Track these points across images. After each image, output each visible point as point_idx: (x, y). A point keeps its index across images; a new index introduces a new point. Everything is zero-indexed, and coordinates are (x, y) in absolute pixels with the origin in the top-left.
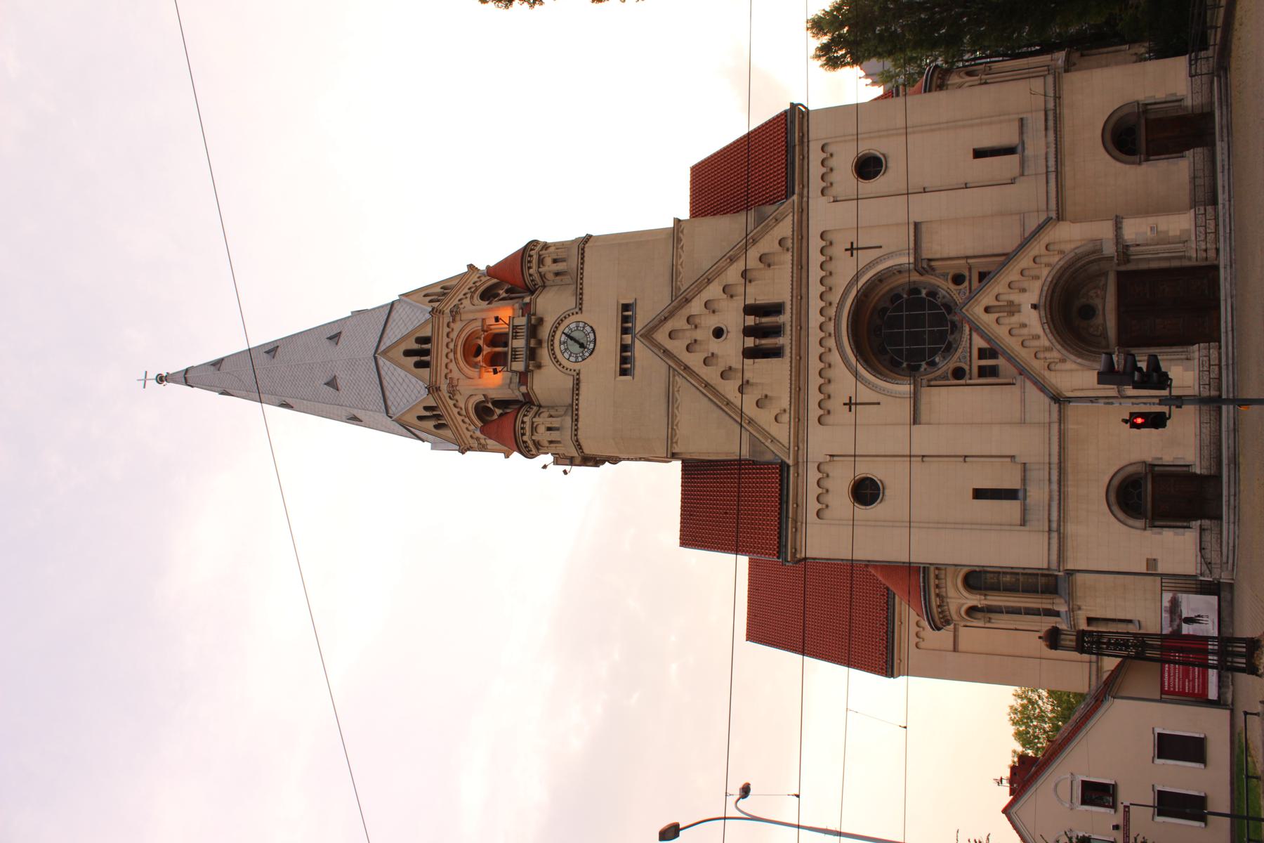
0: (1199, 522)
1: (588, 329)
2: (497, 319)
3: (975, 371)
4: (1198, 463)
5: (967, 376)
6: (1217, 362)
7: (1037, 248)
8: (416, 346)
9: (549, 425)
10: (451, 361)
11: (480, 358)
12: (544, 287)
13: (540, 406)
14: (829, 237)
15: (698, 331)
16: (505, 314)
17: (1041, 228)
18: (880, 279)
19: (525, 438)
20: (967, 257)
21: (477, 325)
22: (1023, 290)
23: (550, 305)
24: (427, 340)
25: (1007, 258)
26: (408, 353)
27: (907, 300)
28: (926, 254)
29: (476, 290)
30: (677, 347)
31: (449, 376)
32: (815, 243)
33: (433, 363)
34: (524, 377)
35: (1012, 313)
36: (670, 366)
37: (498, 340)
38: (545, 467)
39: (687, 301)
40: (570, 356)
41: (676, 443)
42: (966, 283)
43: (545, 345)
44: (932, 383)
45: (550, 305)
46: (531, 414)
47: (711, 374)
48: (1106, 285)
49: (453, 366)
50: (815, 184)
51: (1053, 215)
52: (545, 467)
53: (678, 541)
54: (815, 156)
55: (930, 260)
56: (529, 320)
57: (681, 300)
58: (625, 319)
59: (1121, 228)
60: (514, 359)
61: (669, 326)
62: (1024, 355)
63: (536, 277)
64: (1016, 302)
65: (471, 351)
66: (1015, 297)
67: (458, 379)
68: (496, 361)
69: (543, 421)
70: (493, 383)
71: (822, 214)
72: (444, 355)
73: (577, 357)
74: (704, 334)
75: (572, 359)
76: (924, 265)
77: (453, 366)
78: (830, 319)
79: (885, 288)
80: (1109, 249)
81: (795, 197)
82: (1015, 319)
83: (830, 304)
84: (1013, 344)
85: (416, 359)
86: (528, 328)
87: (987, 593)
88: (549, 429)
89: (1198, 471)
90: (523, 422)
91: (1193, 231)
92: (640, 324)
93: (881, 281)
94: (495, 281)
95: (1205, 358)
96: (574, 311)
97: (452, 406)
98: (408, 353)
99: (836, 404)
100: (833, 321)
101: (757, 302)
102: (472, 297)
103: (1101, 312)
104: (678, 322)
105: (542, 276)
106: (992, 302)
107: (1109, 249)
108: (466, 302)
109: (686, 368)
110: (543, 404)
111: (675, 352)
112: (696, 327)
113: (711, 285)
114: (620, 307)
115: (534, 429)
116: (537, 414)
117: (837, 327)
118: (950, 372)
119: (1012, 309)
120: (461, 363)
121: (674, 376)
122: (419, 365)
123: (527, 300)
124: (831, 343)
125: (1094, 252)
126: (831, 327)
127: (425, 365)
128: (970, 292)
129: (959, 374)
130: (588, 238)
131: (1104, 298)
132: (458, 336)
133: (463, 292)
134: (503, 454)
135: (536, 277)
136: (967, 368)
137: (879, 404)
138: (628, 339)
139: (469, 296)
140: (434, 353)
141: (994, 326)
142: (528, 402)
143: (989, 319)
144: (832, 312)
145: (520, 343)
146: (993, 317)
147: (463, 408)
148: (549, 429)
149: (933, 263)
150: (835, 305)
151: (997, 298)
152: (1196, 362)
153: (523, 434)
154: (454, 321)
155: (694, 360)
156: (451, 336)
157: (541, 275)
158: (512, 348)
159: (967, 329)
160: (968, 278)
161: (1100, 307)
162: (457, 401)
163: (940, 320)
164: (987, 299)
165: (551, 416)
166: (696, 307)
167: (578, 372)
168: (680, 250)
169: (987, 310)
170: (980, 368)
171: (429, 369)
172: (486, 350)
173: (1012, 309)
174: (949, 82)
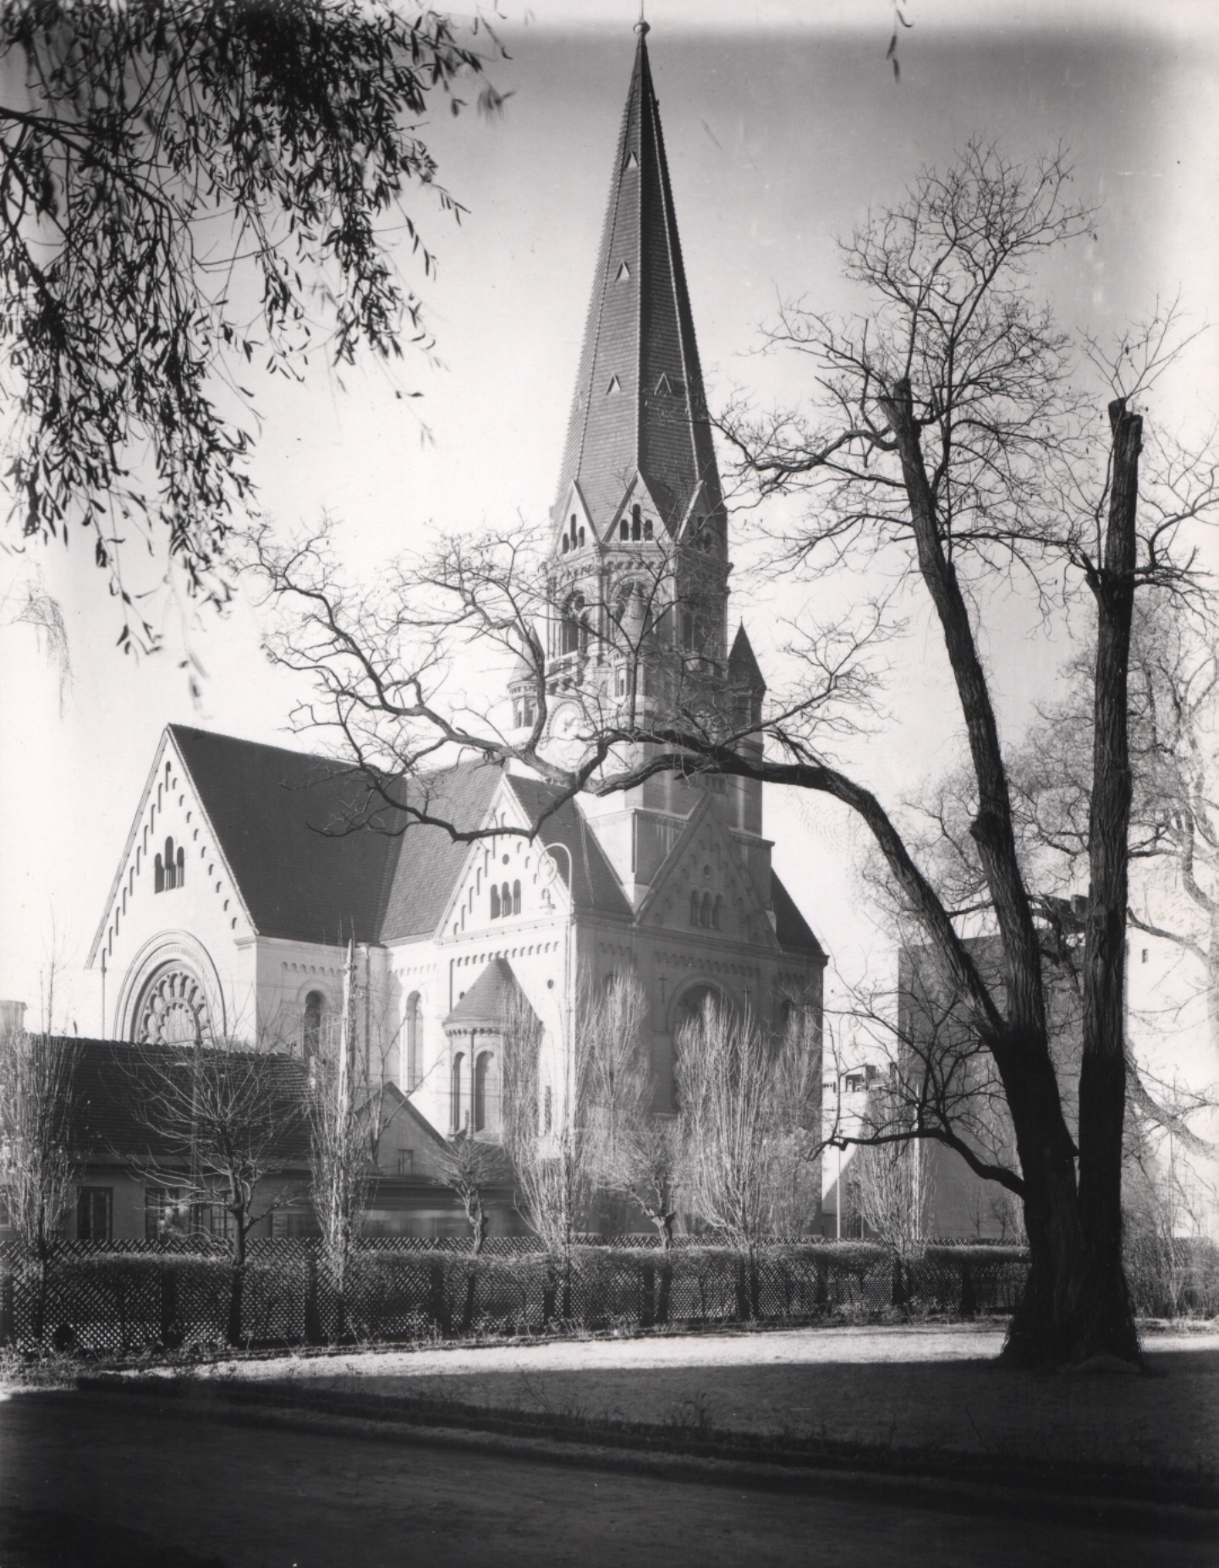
24: (649, 537)
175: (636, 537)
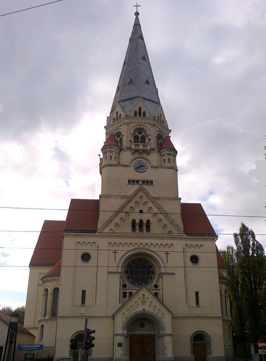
1: (145, 170)
2: (149, 140)
5: (123, 288)
8: (142, 112)
9: (112, 157)
10: (136, 124)
11: (137, 134)
12: (161, 155)
13: (119, 154)
14: (172, 246)
15: (142, 205)
16: (152, 143)
18: (157, 262)
19: (108, 149)
20: (162, 289)
21: (148, 133)
22: (150, 306)
23: (154, 158)
24: (144, 115)
25: (162, 303)
26: (140, 109)
27: (150, 270)
28: (164, 276)
29: (162, 133)
30: (137, 198)
32: (169, 242)
33: (136, 117)
34: (129, 148)
35: (142, 302)
36: (130, 196)
37: (143, 139)
38: (99, 155)
39: (152, 202)
40: (136, 164)
41: (104, 198)
42: (154, 288)
43: (140, 155)
44: (121, 278)
45: (154, 158)
46: (116, 151)
47: (127, 209)
49: (135, 124)
50: (189, 243)
52: (99, 155)
54: (199, 243)
55: (162, 277)
56: (148, 150)
57: (154, 200)
58: (148, 182)
60: (136, 145)
61: (144, 196)
62: (128, 306)
63: (164, 153)
64: (146, 304)
65: (140, 130)
66: (147, 304)
67: (130, 126)
68: (136, 139)
69: (114, 155)
70: (127, 140)
71: (179, 245)
72: (138, 122)
73: (135, 166)
74: (141, 207)
75: (135, 165)
76: (161, 275)
78: (144, 246)
79: (155, 265)
81: (185, 236)
82: (140, 303)
83: (149, 247)
84: (132, 302)
85: (138, 112)
86: (146, 150)
88: (111, 157)
90: (113, 148)
92: (145, 187)
93: (156, 262)
94: (164, 139)
96: (151, 165)
97: (118, 125)
98: (140, 109)
99: (116, 248)
100: (143, 247)
101: (151, 224)
102: (159, 131)
104: (145, 199)
105: (164, 155)
106: (146, 297)
108: (157, 129)
109: (130, 201)
110: (120, 155)
111: (135, 198)
112: (143, 204)
113: (157, 209)
114: (152, 180)
115: (111, 152)
116: (116, 153)
117: (142, 248)
118: (125, 283)
119: (144, 302)
120: (135, 127)
121: (127, 197)
122: (135, 112)
123: (156, 150)
124: (136, 246)
126: (141, 246)
127: (135, 115)
128: (150, 290)
129: (124, 286)
130: (177, 170)
132: (145, 126)
133: (161, 128)
134: (105, 141)
135: (164, 153)
137: (115, 261)
138: (141, 183)
139: (160, 130)
140: (139, 117)
141: (138, 297)
142: (121, 150)
143: (140, 295)
144: (147, 247)
145: (141, 147)
146: (141, 297)
147: (120, 128)
148: (111, 157)
149: (161, 279)
150: (149, 248)
151: (147, 298)
153: (109, 148)
154: (151, 125)
155: (132, 204)
156: (145, 124)
157: (164, 154)
158: (139, 145)
159: (138, 289)
160: (156, 289)
161: (144, 329)
162: (122, 125)
163: (143, 280)
164: (147, 294)
165: (115, 157)
166: (150, 204)
167: (130, 166)
168: (170, 199)
169: (144, 295)
170: (126, 292)
171: (134, 116)
172: (140, 136)
173: (144, 302)
174: (223, 285)
175: (140, 115)
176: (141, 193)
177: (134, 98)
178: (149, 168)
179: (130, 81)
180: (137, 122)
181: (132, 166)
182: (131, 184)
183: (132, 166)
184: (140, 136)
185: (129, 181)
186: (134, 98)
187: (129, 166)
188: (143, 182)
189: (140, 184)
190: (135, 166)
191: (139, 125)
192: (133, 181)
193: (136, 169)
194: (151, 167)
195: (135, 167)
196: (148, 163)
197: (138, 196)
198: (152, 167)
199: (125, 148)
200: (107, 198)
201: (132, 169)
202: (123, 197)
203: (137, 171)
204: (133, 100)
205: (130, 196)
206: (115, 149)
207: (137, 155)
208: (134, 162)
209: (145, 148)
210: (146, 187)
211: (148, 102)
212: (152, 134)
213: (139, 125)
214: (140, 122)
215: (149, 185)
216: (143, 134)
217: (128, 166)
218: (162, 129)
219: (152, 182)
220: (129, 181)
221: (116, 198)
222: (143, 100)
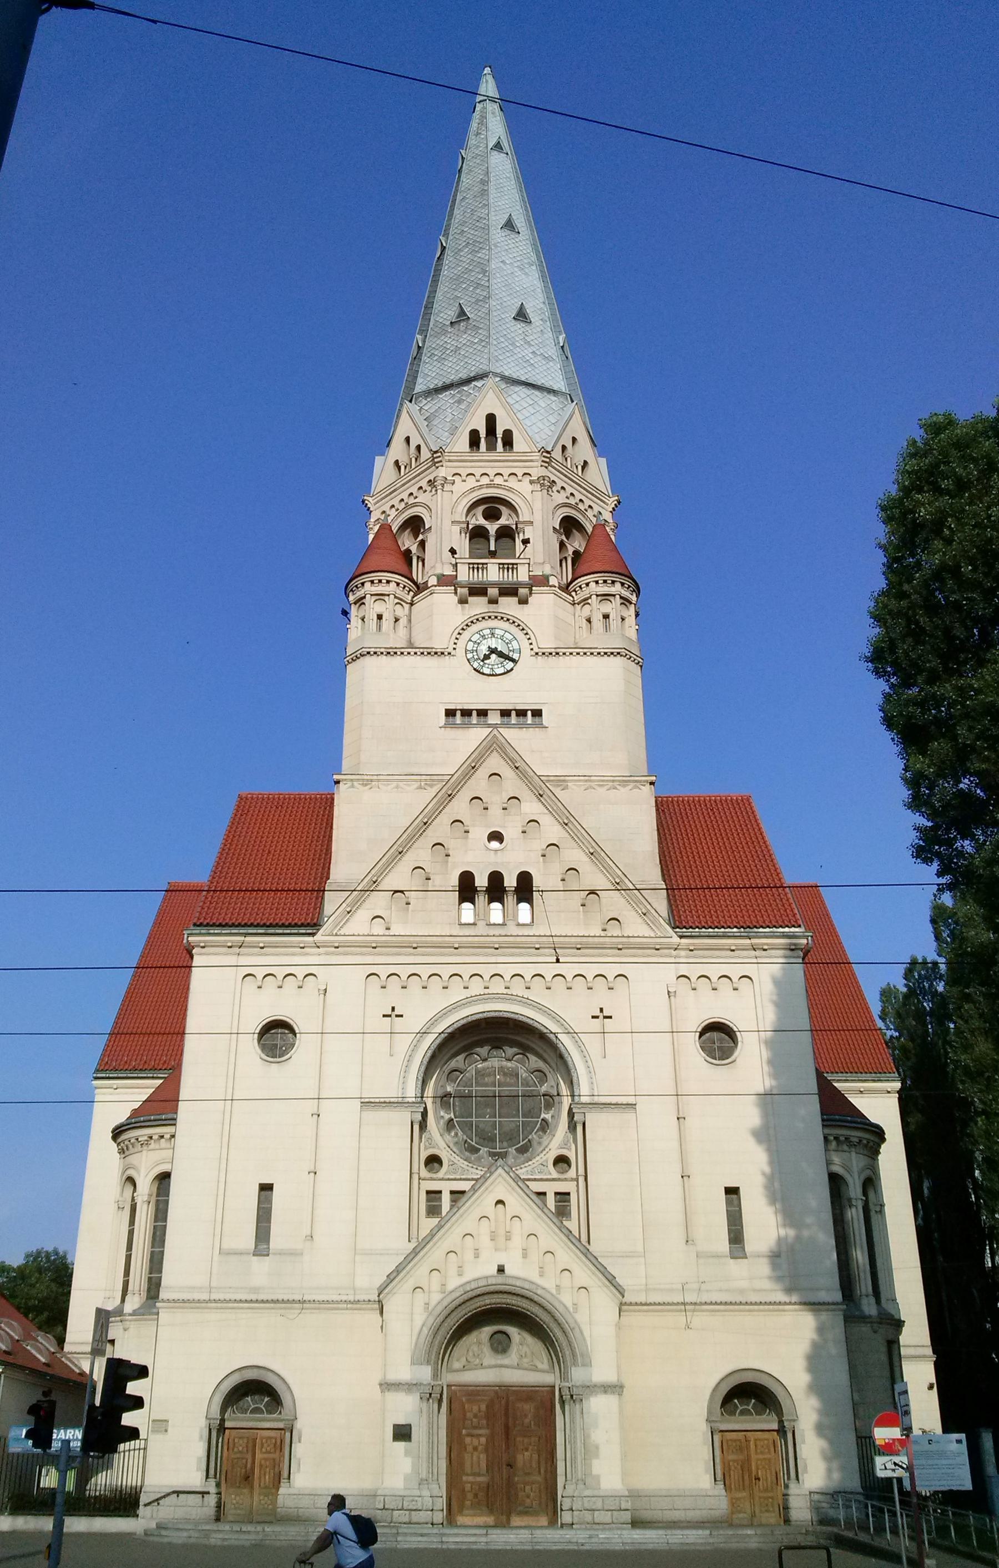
0: (212, 1489)
3: (434, 1186)
4: (291, 1491)
6: (414, 1520)
7: (583, 1274)
17: (611, 1280)
26: (491, 420)
29: (579, 511)
31: (457, 478)
33: (476, 456)
48: (536, 1369)
49: (471, 483)
51: (628, 1298)
53: (245, 792)
59: (605, 1392)
77: (471, 483)
80: (578, 1375)
85: (483, 434)
87: (152, 1205)
89: (281, 1491)
91: (596, 1493)
95: (419, 1504)
98: (491, 420)
103: (499, 1362)
107: (578, 1375)
108: (560, 498)
120: (475, 494)
122: (474, 435)
125: (574, 1355)
131: (518, 1367)
133: (575, 492)
136: (441, 1174)
139: (572, 501)
140: (492, 456)
152: (417, 1493)
154: (531, 482)
156: (513, 478)
175: (491, 447)
176: (495, 762)
177: (468, 381)
178: (526, 659)
179: (459, 316)
180: (478, 472)
181: (460, 651)
182: (454, 726)
183: (460, 651)
184: (492, 528)
185: (450, 713)
186: (468, 381)
187: (449, 654)
188: (505, 713)
189: (489, 726)
190: (472, 651)
191: (488, 486)
192: (466, 713)
193: (476, 665)
194: (533, 653)
195: (470, 656)
196: (520, 635)
197: (483, 773)
198: (537, 654)
199: (433, 581)
200: (361, 788)
201: (458, 665)
202: (430, 779)
203: (478, 672)
204: (465, 388)
205: (453, 775)
206: (393, 585)
207: (478, 605)
208: (466, 635)
209: (509, 577)
210: (514, 736)
211: (523, 391)
212: (537, 518)
213: (488, 486)
214: (491, 472)
215: (528, 726)
216: (503, 521)
217: (442, 653)
218: (578, 496)
219: (537, 713)
220: (450, 713)
221: (397, 787)
222: (503, 386)
